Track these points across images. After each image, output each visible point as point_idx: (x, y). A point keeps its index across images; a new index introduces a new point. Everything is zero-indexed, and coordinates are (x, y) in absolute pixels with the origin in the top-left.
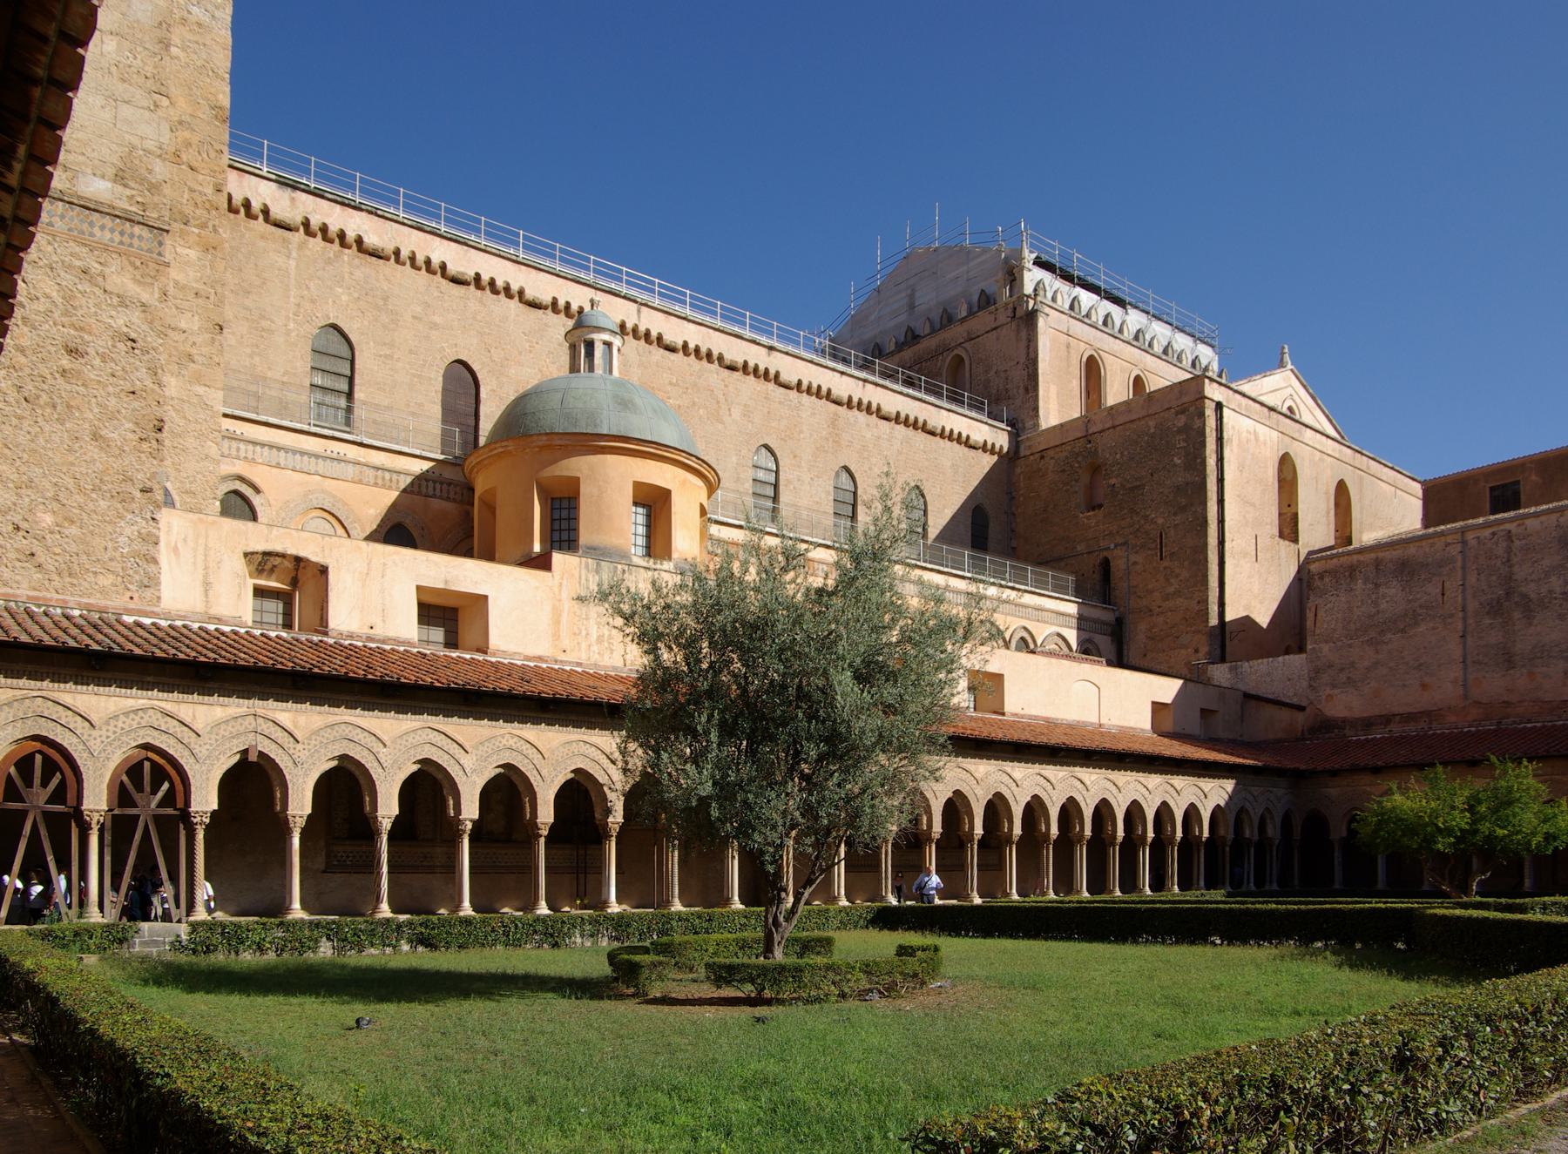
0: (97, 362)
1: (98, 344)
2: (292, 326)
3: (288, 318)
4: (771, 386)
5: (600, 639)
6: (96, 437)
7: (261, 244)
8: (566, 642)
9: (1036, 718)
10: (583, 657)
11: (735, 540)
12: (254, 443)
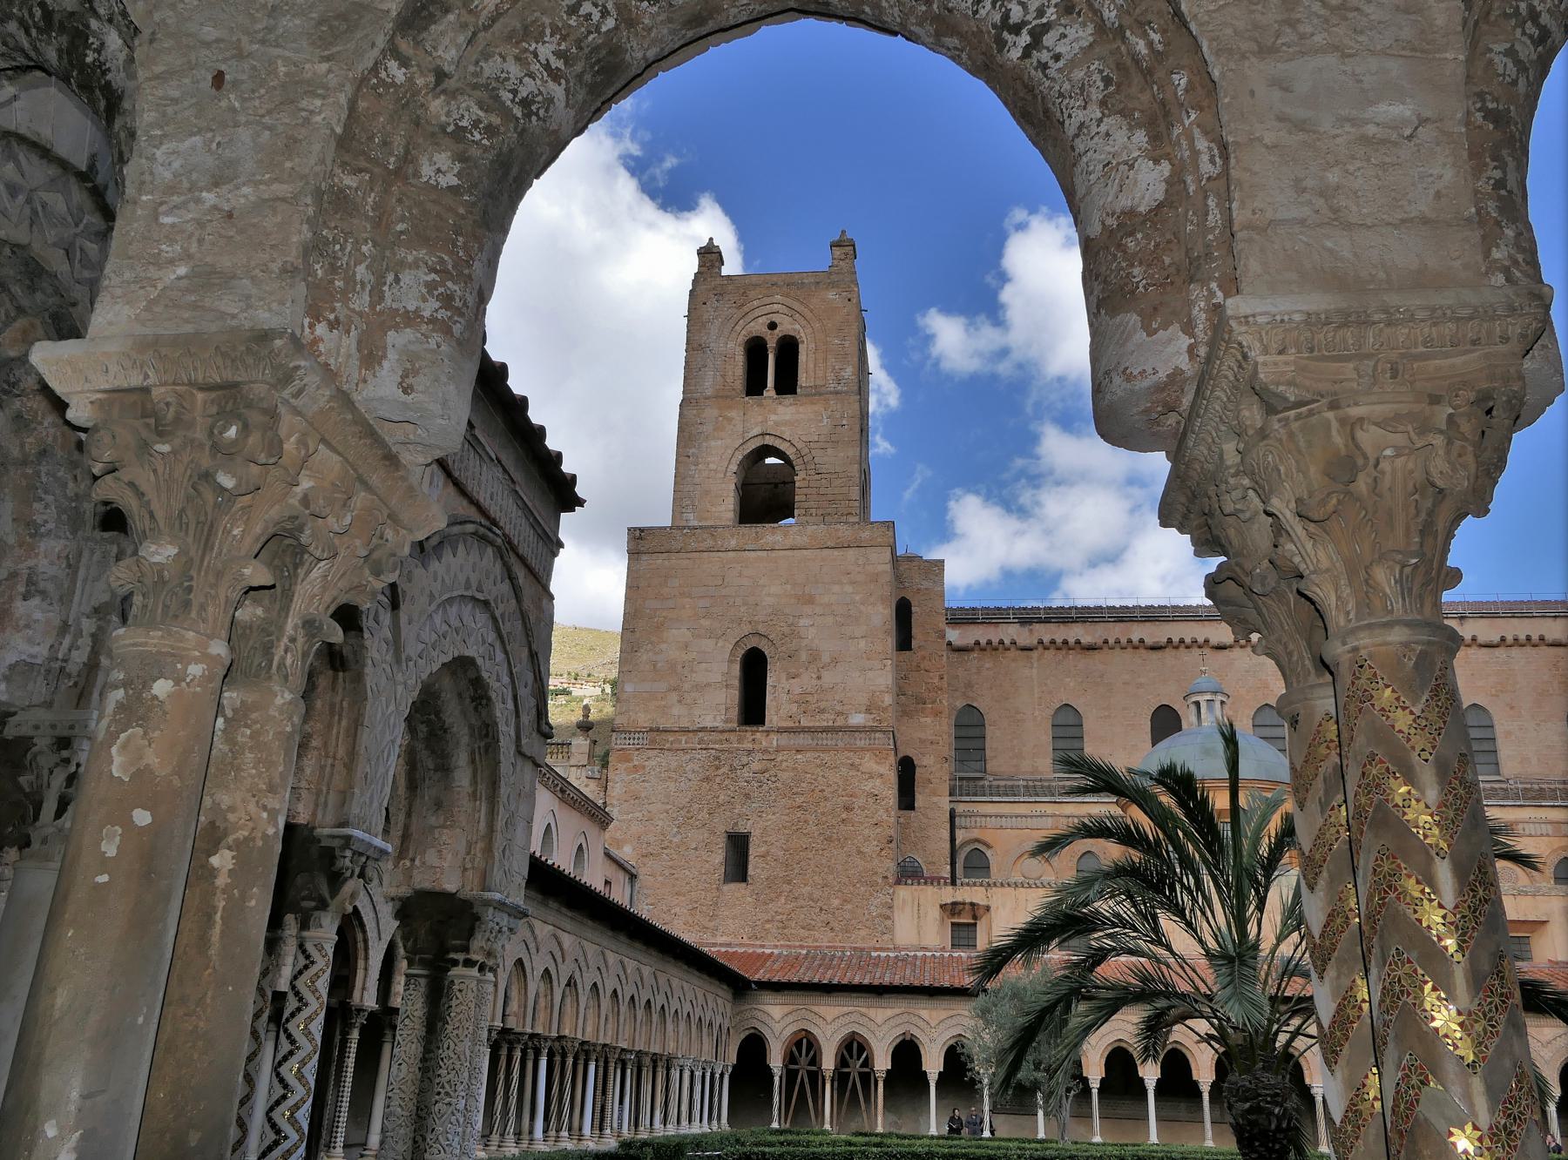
6: (859, 852)
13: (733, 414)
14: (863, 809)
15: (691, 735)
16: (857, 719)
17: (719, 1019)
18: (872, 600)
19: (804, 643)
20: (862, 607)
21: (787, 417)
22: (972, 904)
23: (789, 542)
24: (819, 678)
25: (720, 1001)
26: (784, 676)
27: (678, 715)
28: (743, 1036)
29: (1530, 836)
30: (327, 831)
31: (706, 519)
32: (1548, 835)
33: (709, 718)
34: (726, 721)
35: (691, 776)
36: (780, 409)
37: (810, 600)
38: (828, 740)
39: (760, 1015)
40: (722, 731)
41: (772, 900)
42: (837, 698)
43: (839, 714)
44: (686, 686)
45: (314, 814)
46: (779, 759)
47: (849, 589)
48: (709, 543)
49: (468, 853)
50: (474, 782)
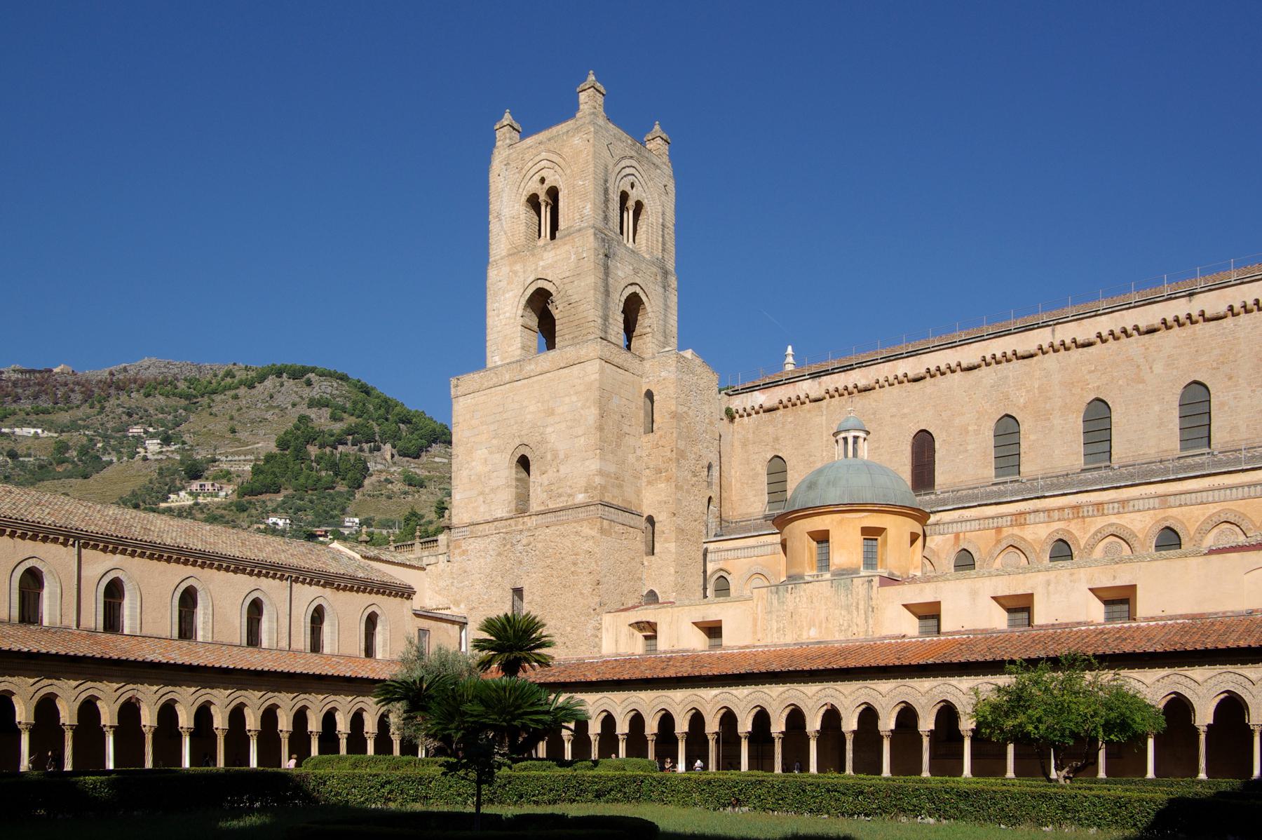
0: (581, 565)
1: (581, 558)
2: (824, 454)
3: (822, 451)
4: (1201, 326)
5: (778, 630)
6: (581, 594)
7: (808, 415)
8: (760, 636)
9: (974, 632)
10: (768, 641)
11: (1023, 510)
12: (728, 550)
13: (518, 267)
14: (583, 563)
15: (490, 524)
16: (580, 498)
18: (588, 404)
19: (549, 446)
20: (582, 411)
21: (550, 261)
22: (648, 622)
23: (539, 370)
24: (558, 471)
27: (483, 513)
29: (1139, 511)
31: (506, 358)
32: (1154, 508)
33: (500, 511)
34: (510, 511)
35: (492, 553)
36: (546, 255)
37: (551, 412)
38: (563, 516)
40: (506, 520)
42: (568, 484)
43: (570, 495)
44: (487, 490)
47: (574, 398)
48: (495, 380)
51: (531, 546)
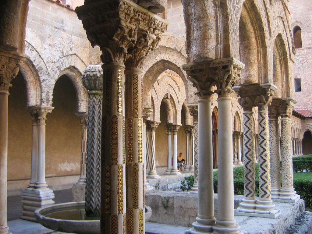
17: (298, 128)
25: (298, 123)
26: (306, 33)
28: (305, 131)
30: (263, 85)
39: (309, 126)
41: (309, 95)
45: (259, 80)
46: (307, 57)
49: (282, 88)
50: (281, 69)
51: (304, 62)
